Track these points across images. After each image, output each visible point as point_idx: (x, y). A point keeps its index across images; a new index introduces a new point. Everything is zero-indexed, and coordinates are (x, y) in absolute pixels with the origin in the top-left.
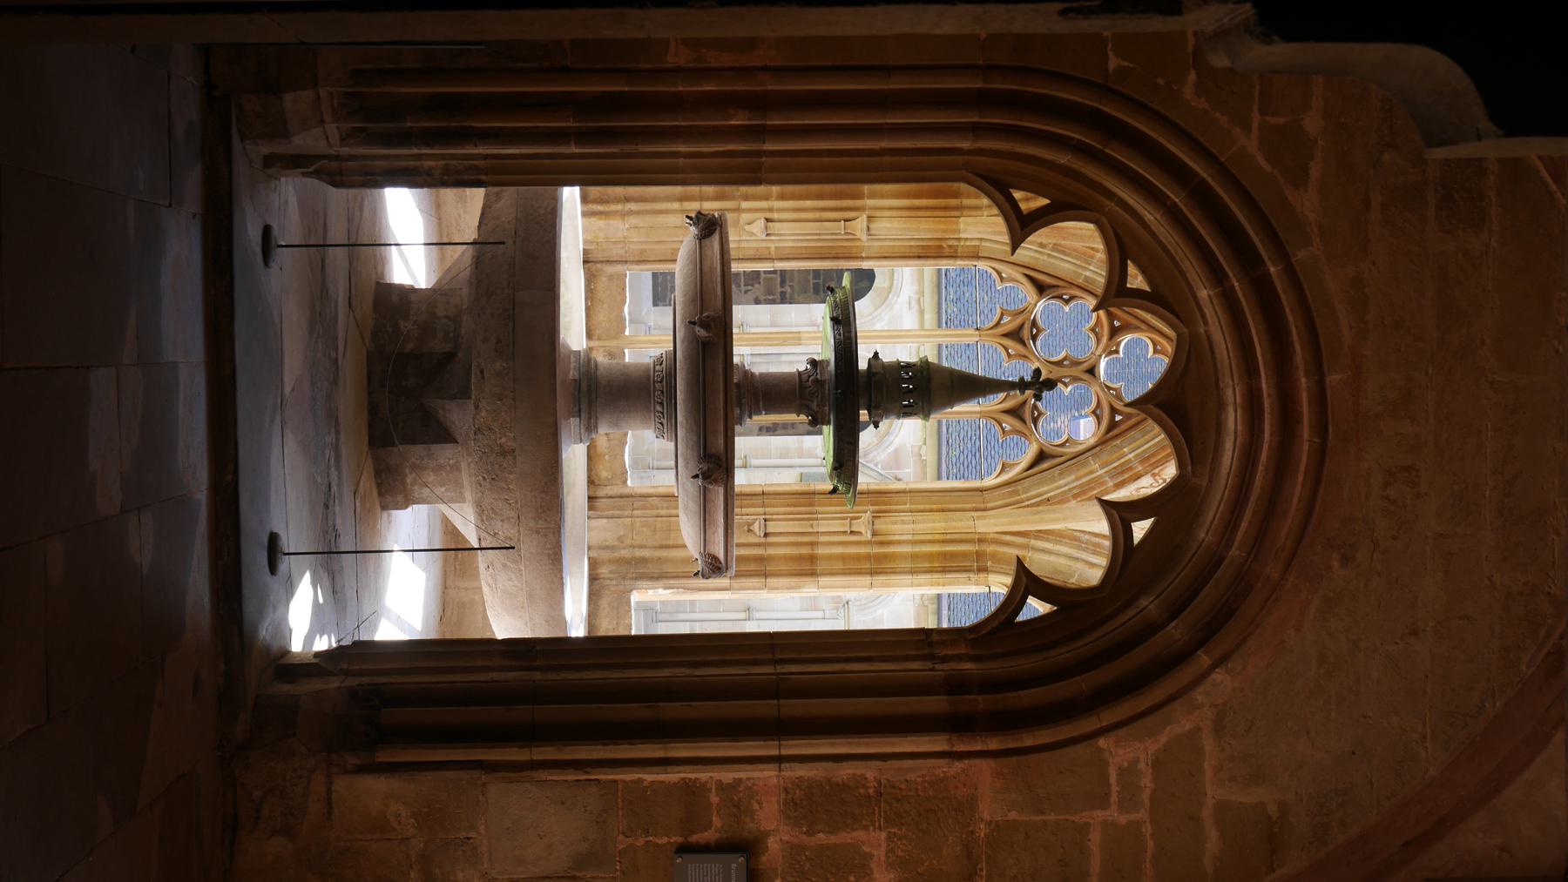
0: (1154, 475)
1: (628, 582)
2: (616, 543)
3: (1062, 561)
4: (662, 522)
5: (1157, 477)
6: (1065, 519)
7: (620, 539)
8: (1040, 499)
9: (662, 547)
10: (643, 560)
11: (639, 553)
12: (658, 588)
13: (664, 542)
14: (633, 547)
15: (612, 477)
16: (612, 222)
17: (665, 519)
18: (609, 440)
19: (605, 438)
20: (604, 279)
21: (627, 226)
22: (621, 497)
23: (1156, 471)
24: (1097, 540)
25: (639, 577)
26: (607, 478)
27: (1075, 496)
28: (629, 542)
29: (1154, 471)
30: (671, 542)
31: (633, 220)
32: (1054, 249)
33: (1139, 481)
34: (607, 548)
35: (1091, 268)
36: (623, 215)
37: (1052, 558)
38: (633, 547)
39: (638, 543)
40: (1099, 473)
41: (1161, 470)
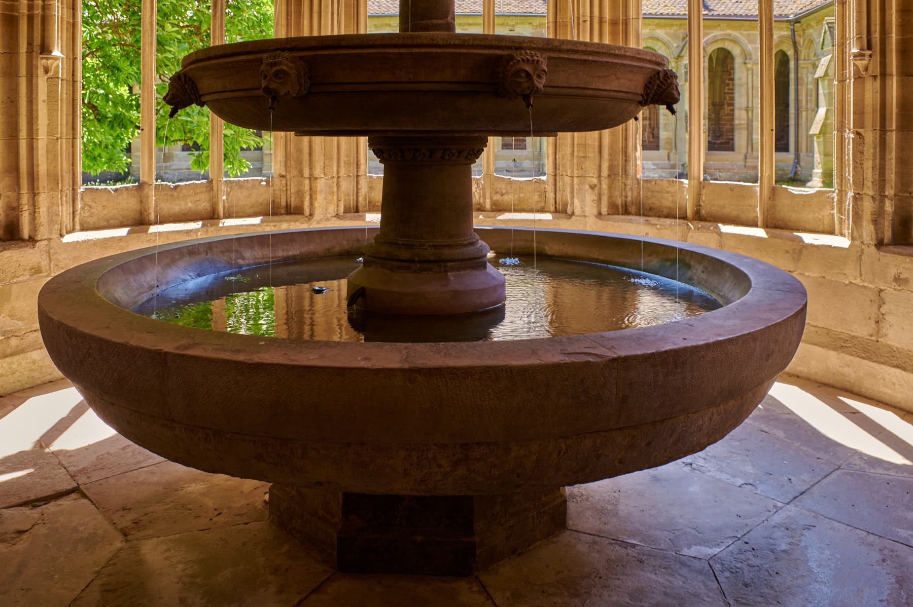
1: (629, 182)
2: (596, 191)
4: (578, 151)
7: (592, 187)
9: (600, 152)
10: (611, 167)
11: (605, 172)
12: (635, 156)
13: (597, 150)
14: (600, 176)
15: (538, 191)
16: (319, 188)
17: (576, 149)
18: (507, 193)
19: (506, 197)
20: (373, 194)
21: (323, 176)
22: (555, 185)
25: (625, 171)
26: (539, 196)
28: (595, 181)
30: (597, 144)
31: (318, 172)
34: (600, 199)
36: (312, 178)
38: (600, 176)
39: (596, 172)
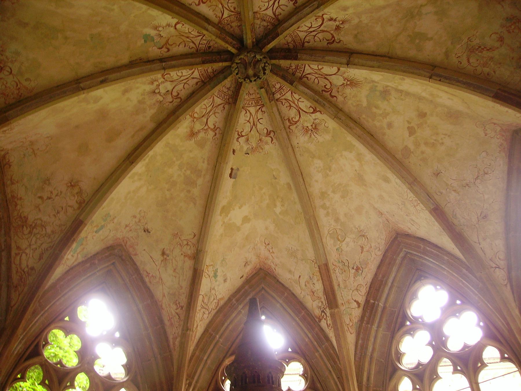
0: (320, 320)
3: (373, 367)
5: (321, 318)
6: (350, 363)
8: (338, 383)
23: (317, 320)
24: (359, 347)
27: (335, 363)
29: (318, 321)
32: (193, 378)
33: (324, 328)
35: (205, 358)
37: (373, 372)
40: (321, 351)
41: (316, 317)
